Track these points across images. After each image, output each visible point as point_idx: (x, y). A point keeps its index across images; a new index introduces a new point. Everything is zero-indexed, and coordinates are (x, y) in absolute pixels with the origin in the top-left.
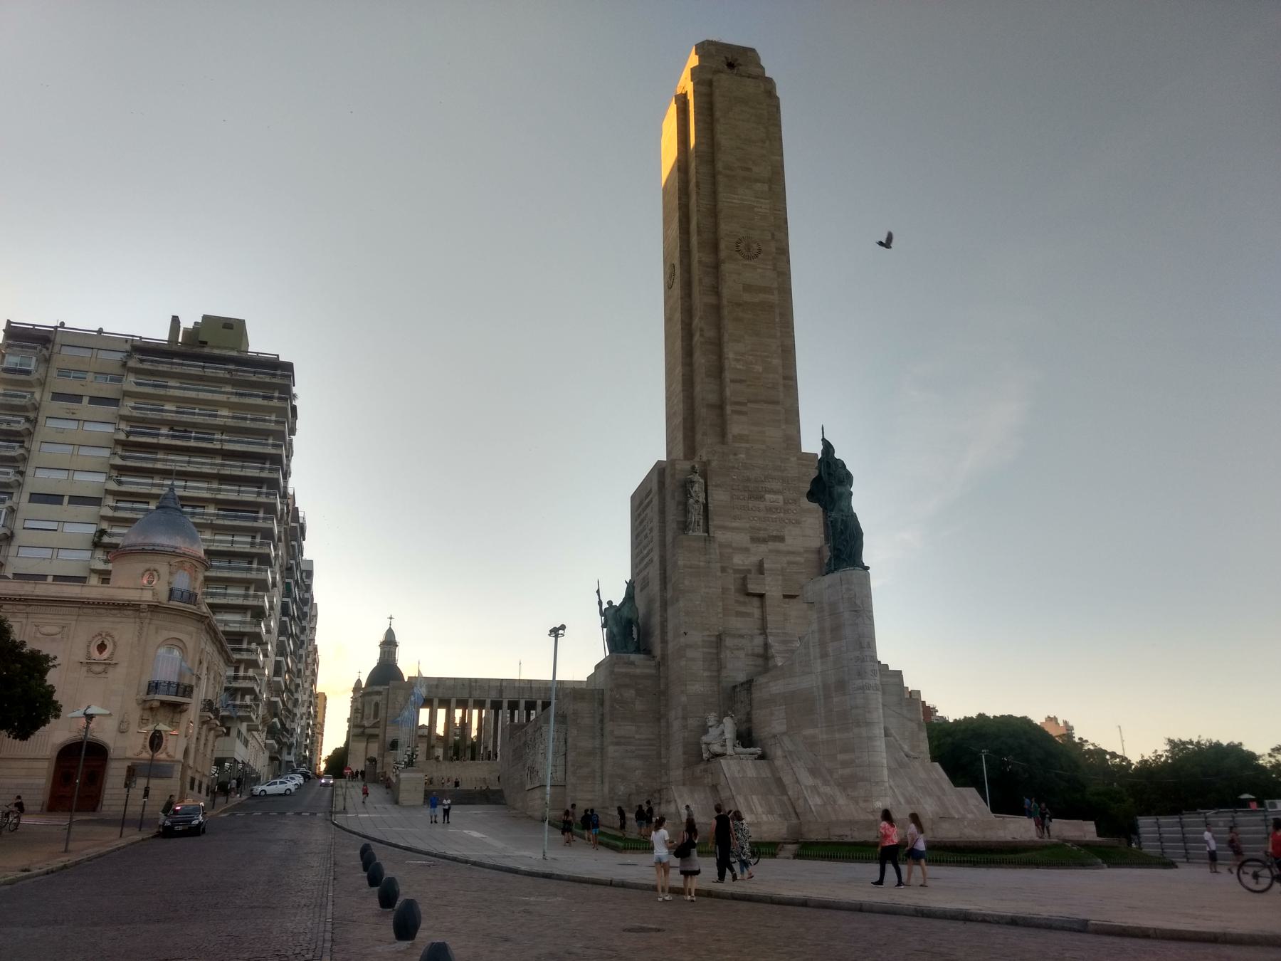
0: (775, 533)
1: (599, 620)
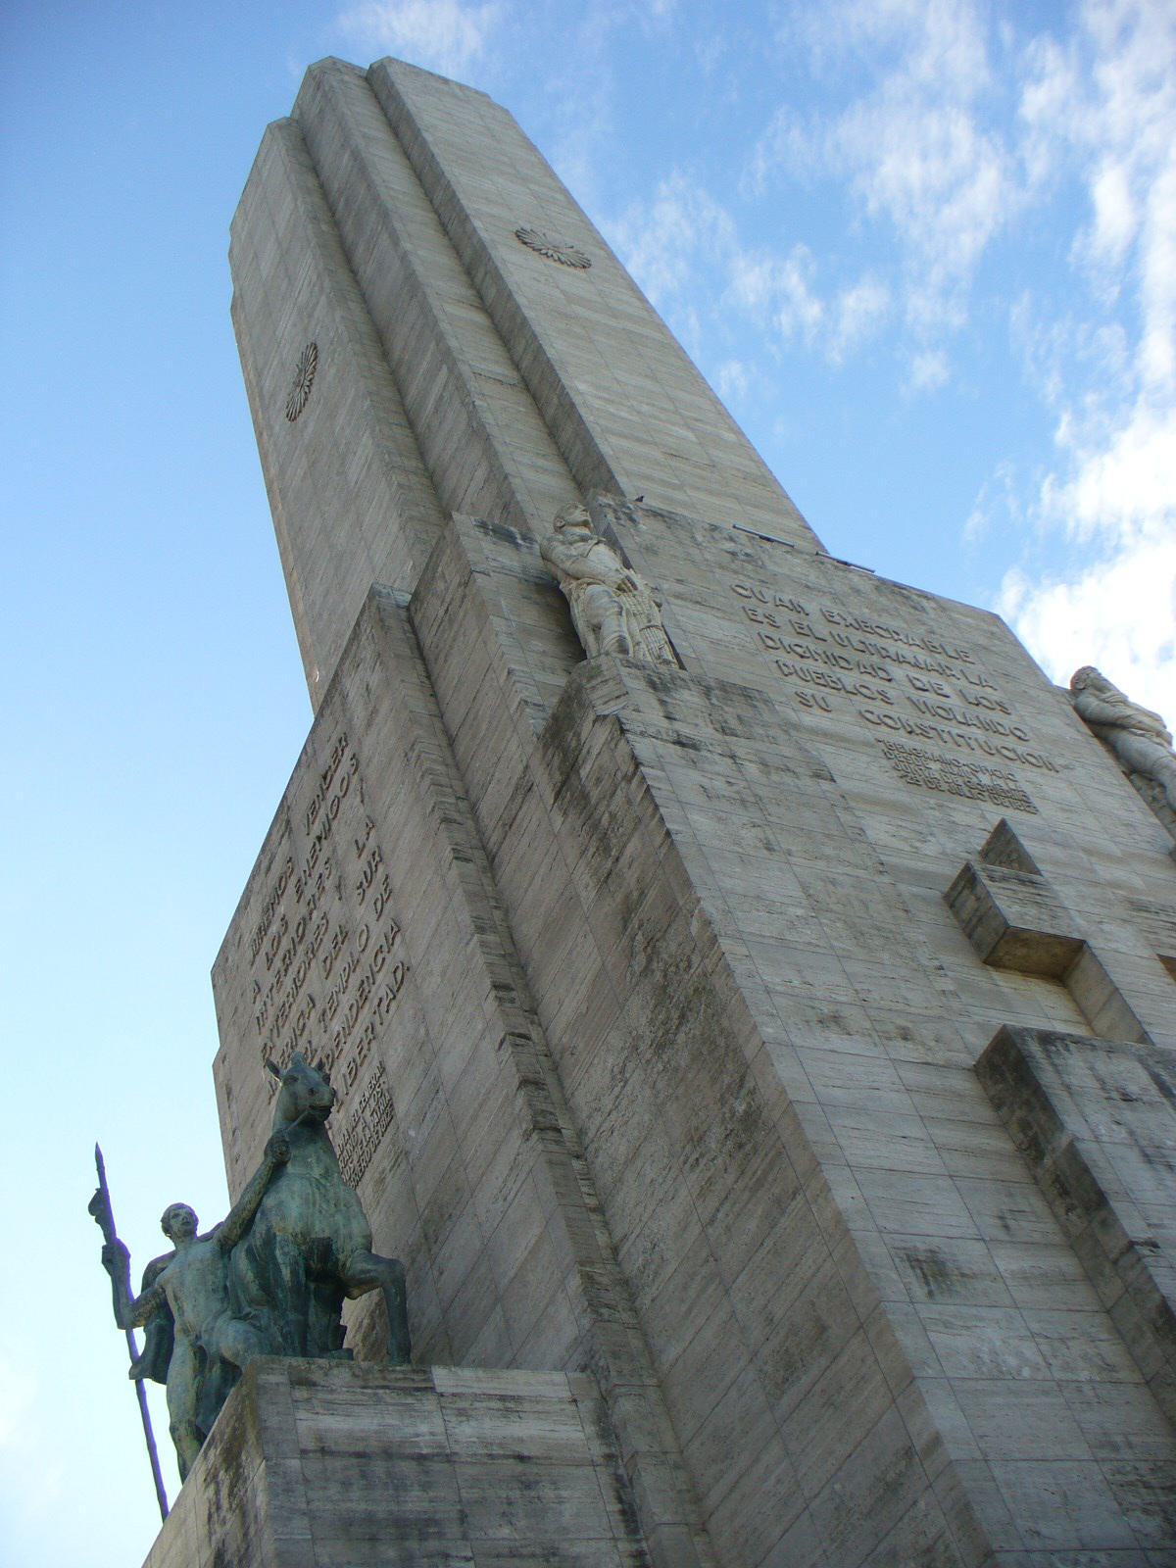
0: (985, 779)
1: (113, 1349)
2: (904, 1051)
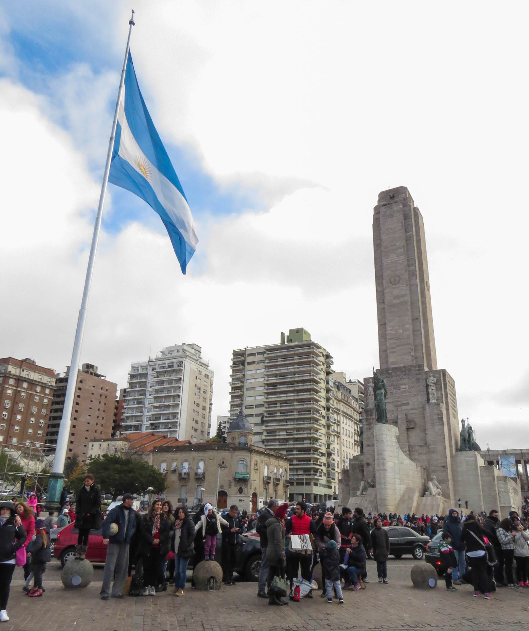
0: (405, 402)
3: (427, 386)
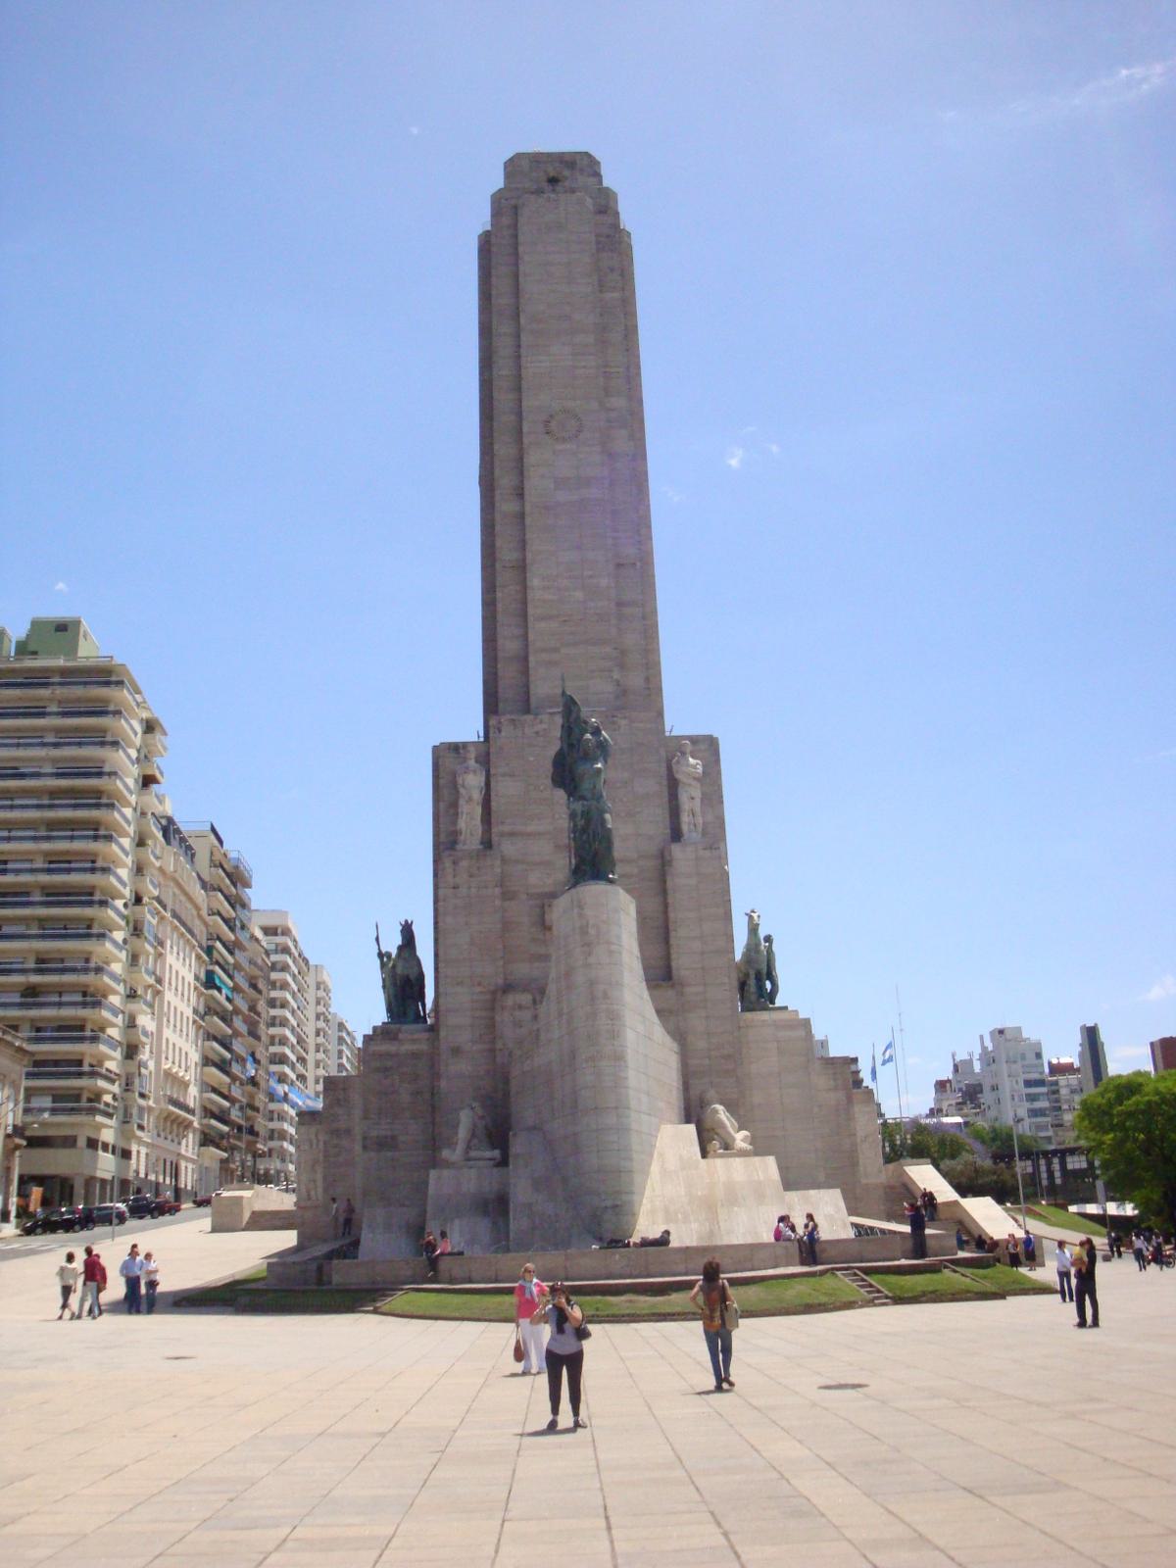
2: (478, 989)
3: (673, 785)
